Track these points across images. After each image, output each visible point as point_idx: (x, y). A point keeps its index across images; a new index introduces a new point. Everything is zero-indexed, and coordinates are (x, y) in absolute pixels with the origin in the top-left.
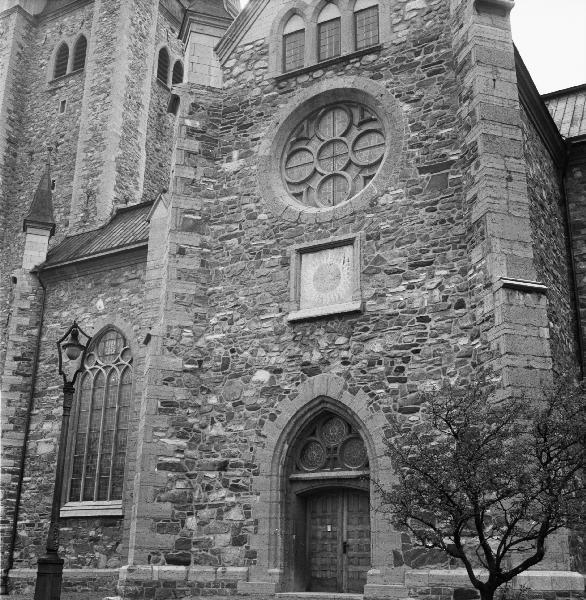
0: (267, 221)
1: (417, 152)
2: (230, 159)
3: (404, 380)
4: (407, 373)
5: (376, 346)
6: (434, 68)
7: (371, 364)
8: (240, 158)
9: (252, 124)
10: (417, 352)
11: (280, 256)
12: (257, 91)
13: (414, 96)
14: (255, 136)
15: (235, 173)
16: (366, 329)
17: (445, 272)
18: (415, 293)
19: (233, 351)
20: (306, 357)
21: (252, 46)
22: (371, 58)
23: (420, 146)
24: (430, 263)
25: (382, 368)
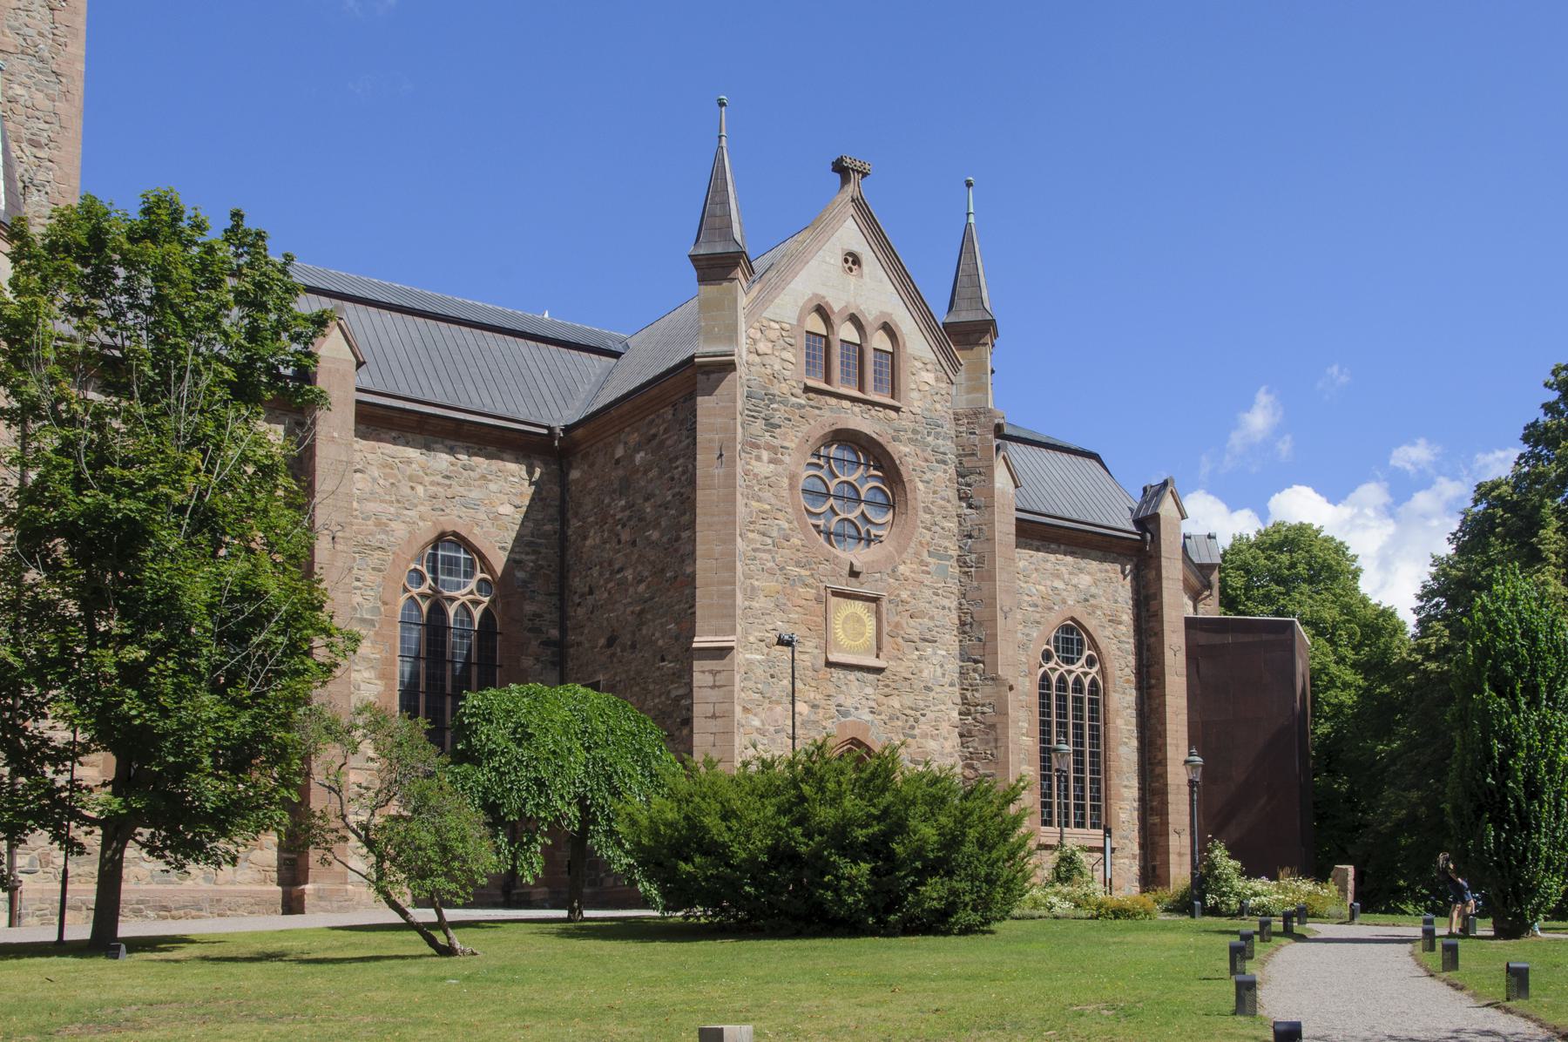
0: (801, 548)
1: (928, 535)
2: (758, 458)
3: (914, 737)
4: (916, 732)
5: (895, 702)
6: (941, 456)
7: (891, 718)
8: (771, 461)
9: (780, 426)
10: (923, 715)
11: (814, 591)
12: (785, 388)
13: (925, 477)
14: (786, 444)
15: (766, 478)
16: (887, 686)
17: (944, 653)
18: (923, 664)
19: (772, 676)
20: (841, 699)
21: (777, 326)
22: (893, 414)
23: (929, 530)
24: (936, 641)
25: (900, 723)
